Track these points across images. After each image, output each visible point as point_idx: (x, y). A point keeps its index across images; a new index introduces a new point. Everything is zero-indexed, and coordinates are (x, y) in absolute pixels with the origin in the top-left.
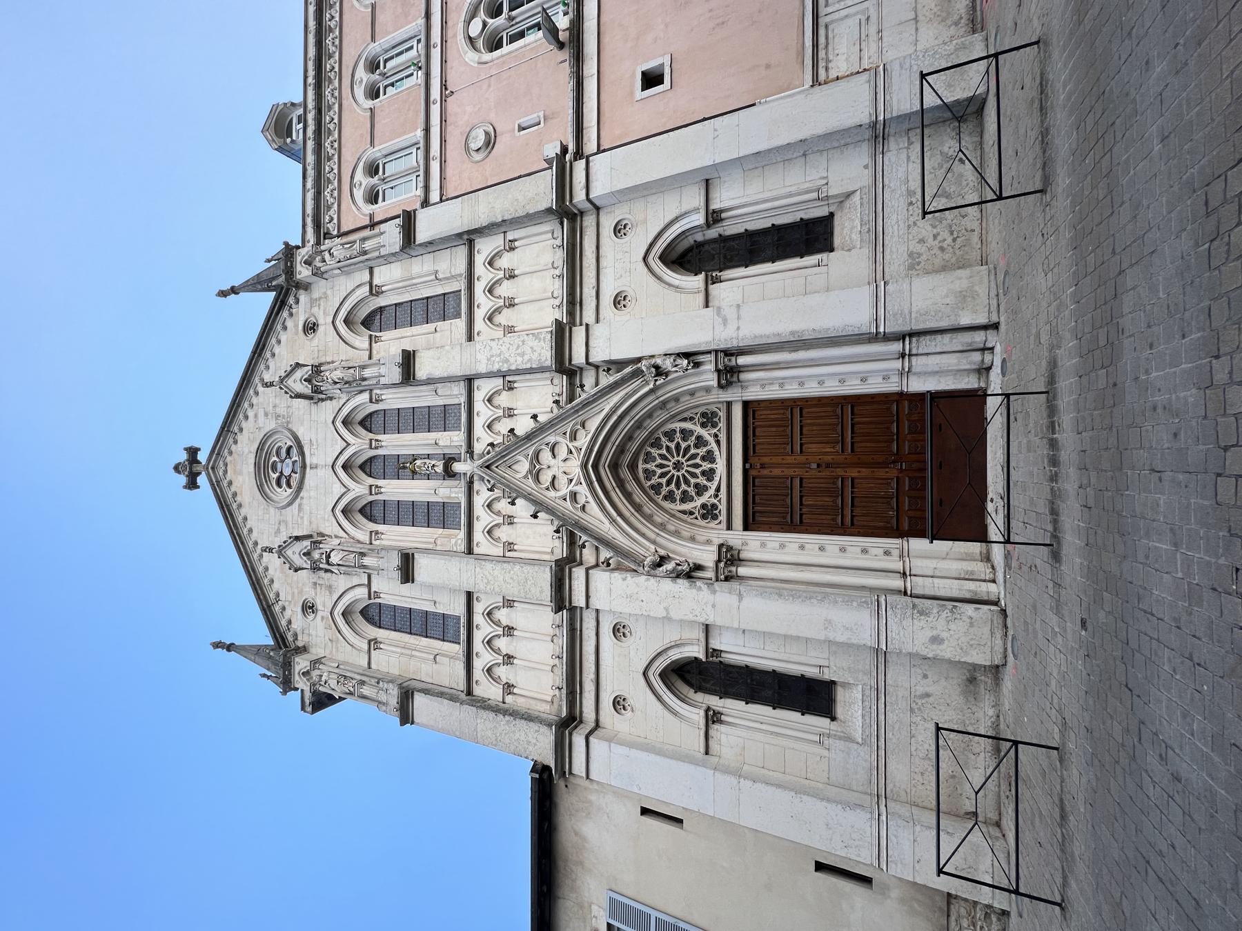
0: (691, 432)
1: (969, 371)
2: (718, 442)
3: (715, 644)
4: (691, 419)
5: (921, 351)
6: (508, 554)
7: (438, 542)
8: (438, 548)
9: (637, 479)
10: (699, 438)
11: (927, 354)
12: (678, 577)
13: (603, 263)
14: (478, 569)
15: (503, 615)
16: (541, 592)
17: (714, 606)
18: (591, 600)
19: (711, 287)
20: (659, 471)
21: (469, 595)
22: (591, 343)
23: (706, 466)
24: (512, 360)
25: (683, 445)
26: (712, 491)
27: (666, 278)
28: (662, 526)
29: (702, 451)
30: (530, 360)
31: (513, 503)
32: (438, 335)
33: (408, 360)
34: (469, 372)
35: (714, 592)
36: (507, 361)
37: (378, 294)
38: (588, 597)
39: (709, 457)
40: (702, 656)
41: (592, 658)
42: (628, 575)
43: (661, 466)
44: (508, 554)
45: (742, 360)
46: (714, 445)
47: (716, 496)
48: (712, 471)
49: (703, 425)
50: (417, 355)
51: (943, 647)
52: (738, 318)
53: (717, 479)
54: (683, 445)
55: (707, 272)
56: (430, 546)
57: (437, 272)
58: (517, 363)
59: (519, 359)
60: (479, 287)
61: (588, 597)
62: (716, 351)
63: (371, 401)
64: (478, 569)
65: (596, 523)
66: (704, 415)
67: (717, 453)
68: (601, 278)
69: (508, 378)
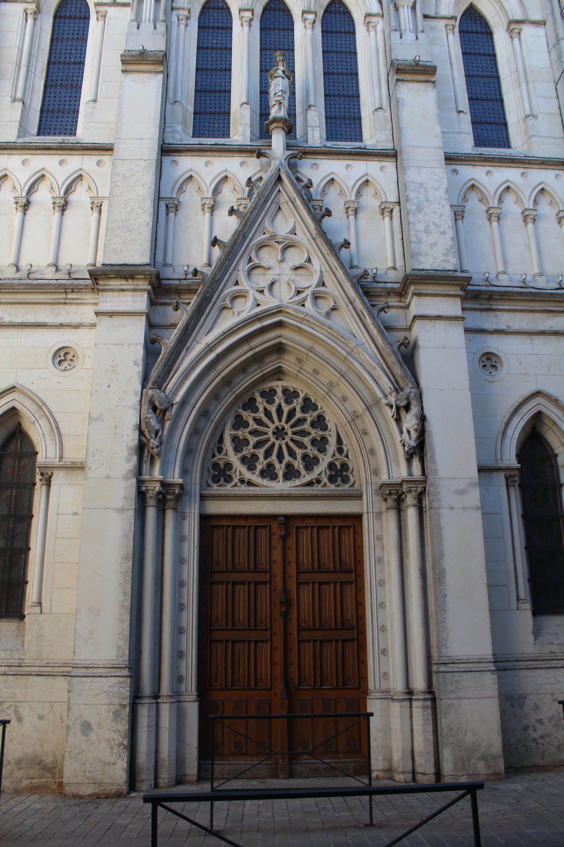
0: (323, 450)
1: (389, 760)
2: (310, 484)
3: (58, 479)
4: (340, 450)
5: (415, 710)
6: (163, 204)
7: (177, 107)
8: (169, 106)
9: (265, 378)
10: (316, 461)
11: (411, 717)
12: (141, 433)
13: (538, 340)
14: (143, 164)
15: (80, 196)
16: (116, 252)
17: (108, 477)
18: (106, 320)
19: (502, 475)
20: (273, 409)
21: (107, 149)
22: (440, 324)
23: (280, 469)
24: (420, 216)
25: (306, 441)
26: (248, 475)
27: (516, 419)
28: (204, 413)
29: (298, 464)
30: (420, 241)
31: (232, 211)
32: (455, 114)
33: (422, 71)
34: (407, 155)
35: (126, 478)
36: (419, 209)
37: (510, 31)
38: (111, 314)
39: (290, 473)
40: (41, 459)
41: (30, 319)
42: (140, 369)
43: (279, 411)
44: (163, 204)
45: (411, 514)
46: (308, 478)
47: (242, 481)
48: (274, 477)
49: (331, 466)
50: (429, 86)
51: (79, 735)
52: (464, 508)
53: (265, 482)
54: (306, 441)
55: (520, 470)
56: (170, 95)
57: (535, 117)
58: (418, 222)
59: (421, 227)
60: (512, 174)
61: (111, 314)
62: (425, 482)
63: (368, 15)
64: (143, 164)
65: (208, 325)
66: (345, 466)
67: (298, 482)
68: (520, 338)
69: (396, 213)
